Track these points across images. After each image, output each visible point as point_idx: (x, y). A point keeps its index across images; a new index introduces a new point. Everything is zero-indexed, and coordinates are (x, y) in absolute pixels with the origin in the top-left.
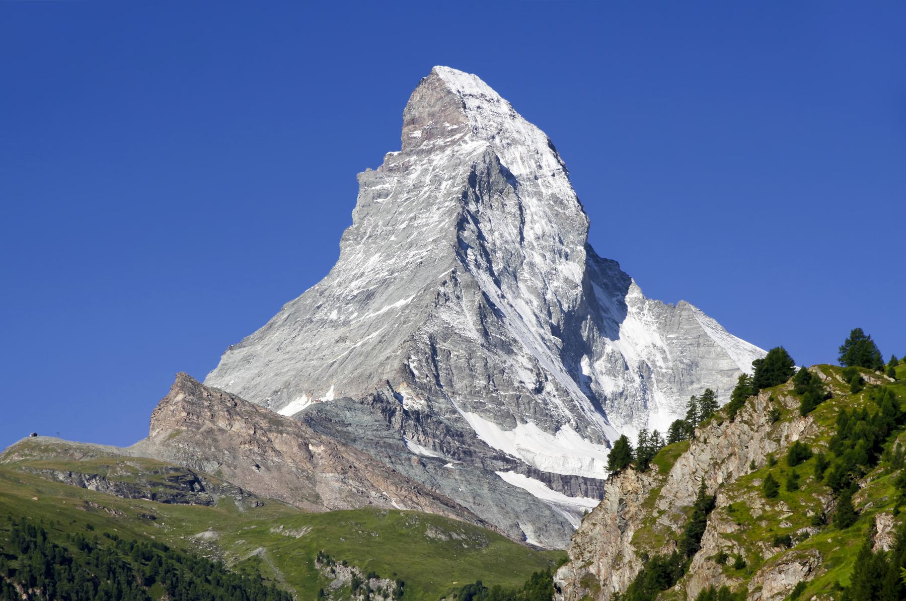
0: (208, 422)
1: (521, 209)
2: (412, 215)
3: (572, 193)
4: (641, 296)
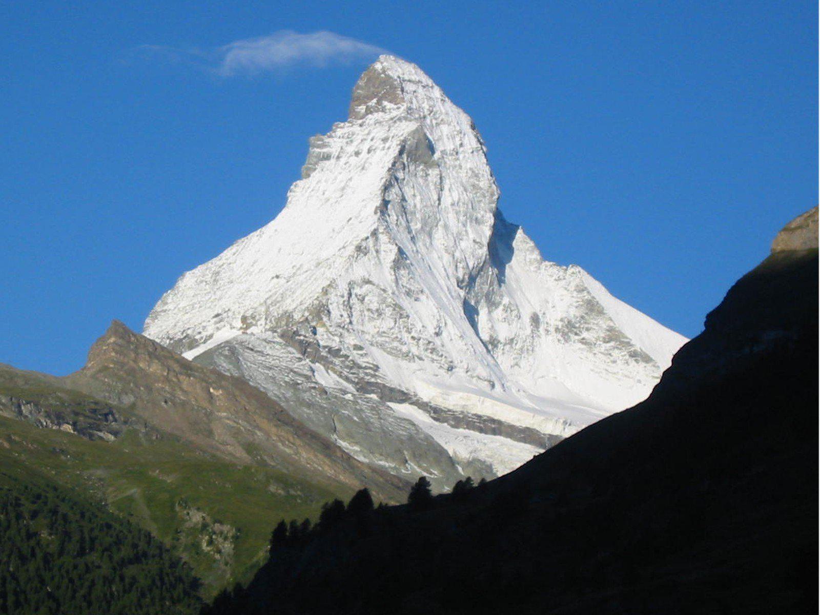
0: (131, 362)
3: (487, 168)
4: (539, 257)
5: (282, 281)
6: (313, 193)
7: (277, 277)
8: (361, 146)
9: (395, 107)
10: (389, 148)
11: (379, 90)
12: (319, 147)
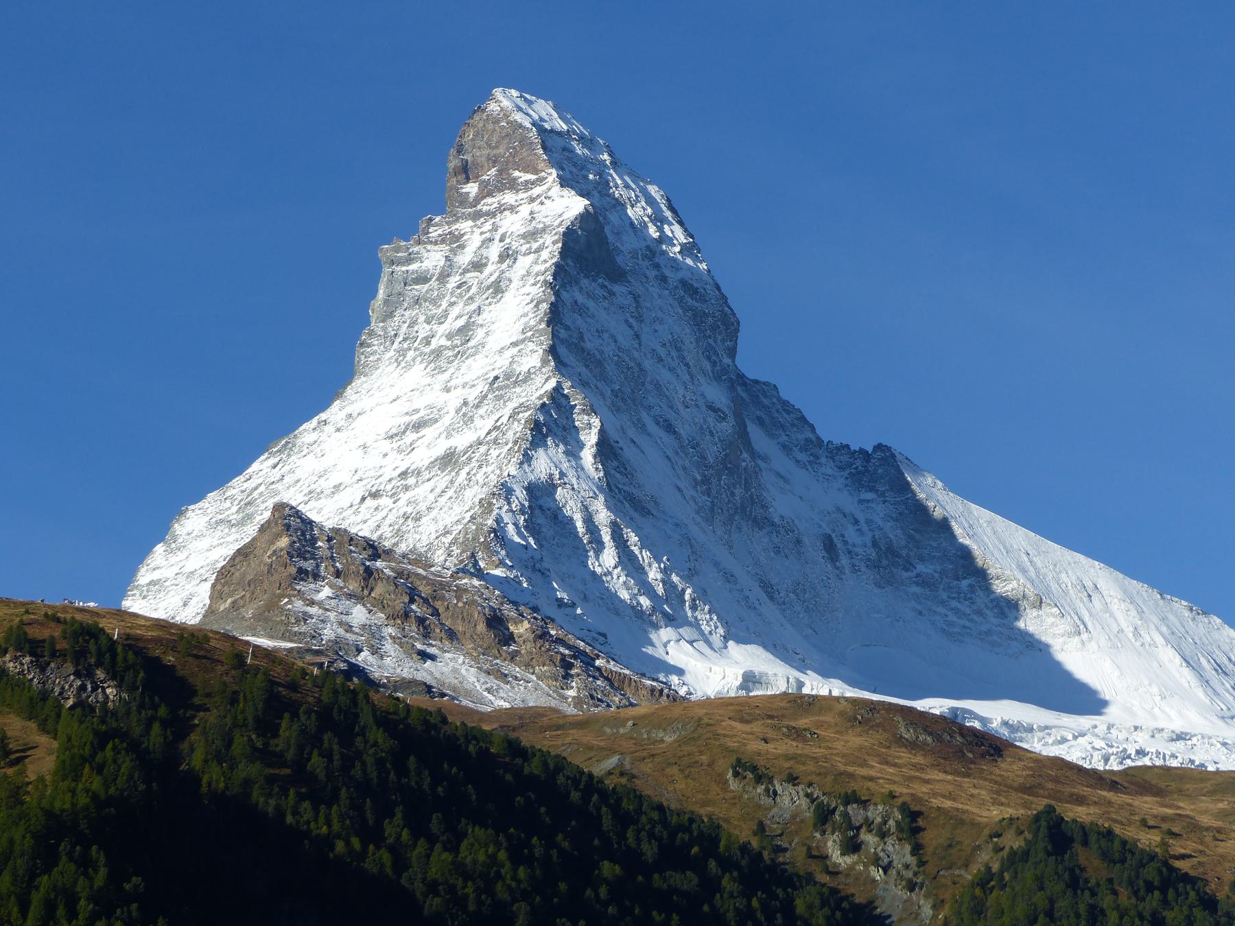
1: (636, 298)
2: (473, 307)
5: (385, 501)
6: (405, 345)
7: (375, 495)
8: (484, 252)
9: (533, 177)
10: (538, 251)
11: (501, 150)
12: (400, 262)
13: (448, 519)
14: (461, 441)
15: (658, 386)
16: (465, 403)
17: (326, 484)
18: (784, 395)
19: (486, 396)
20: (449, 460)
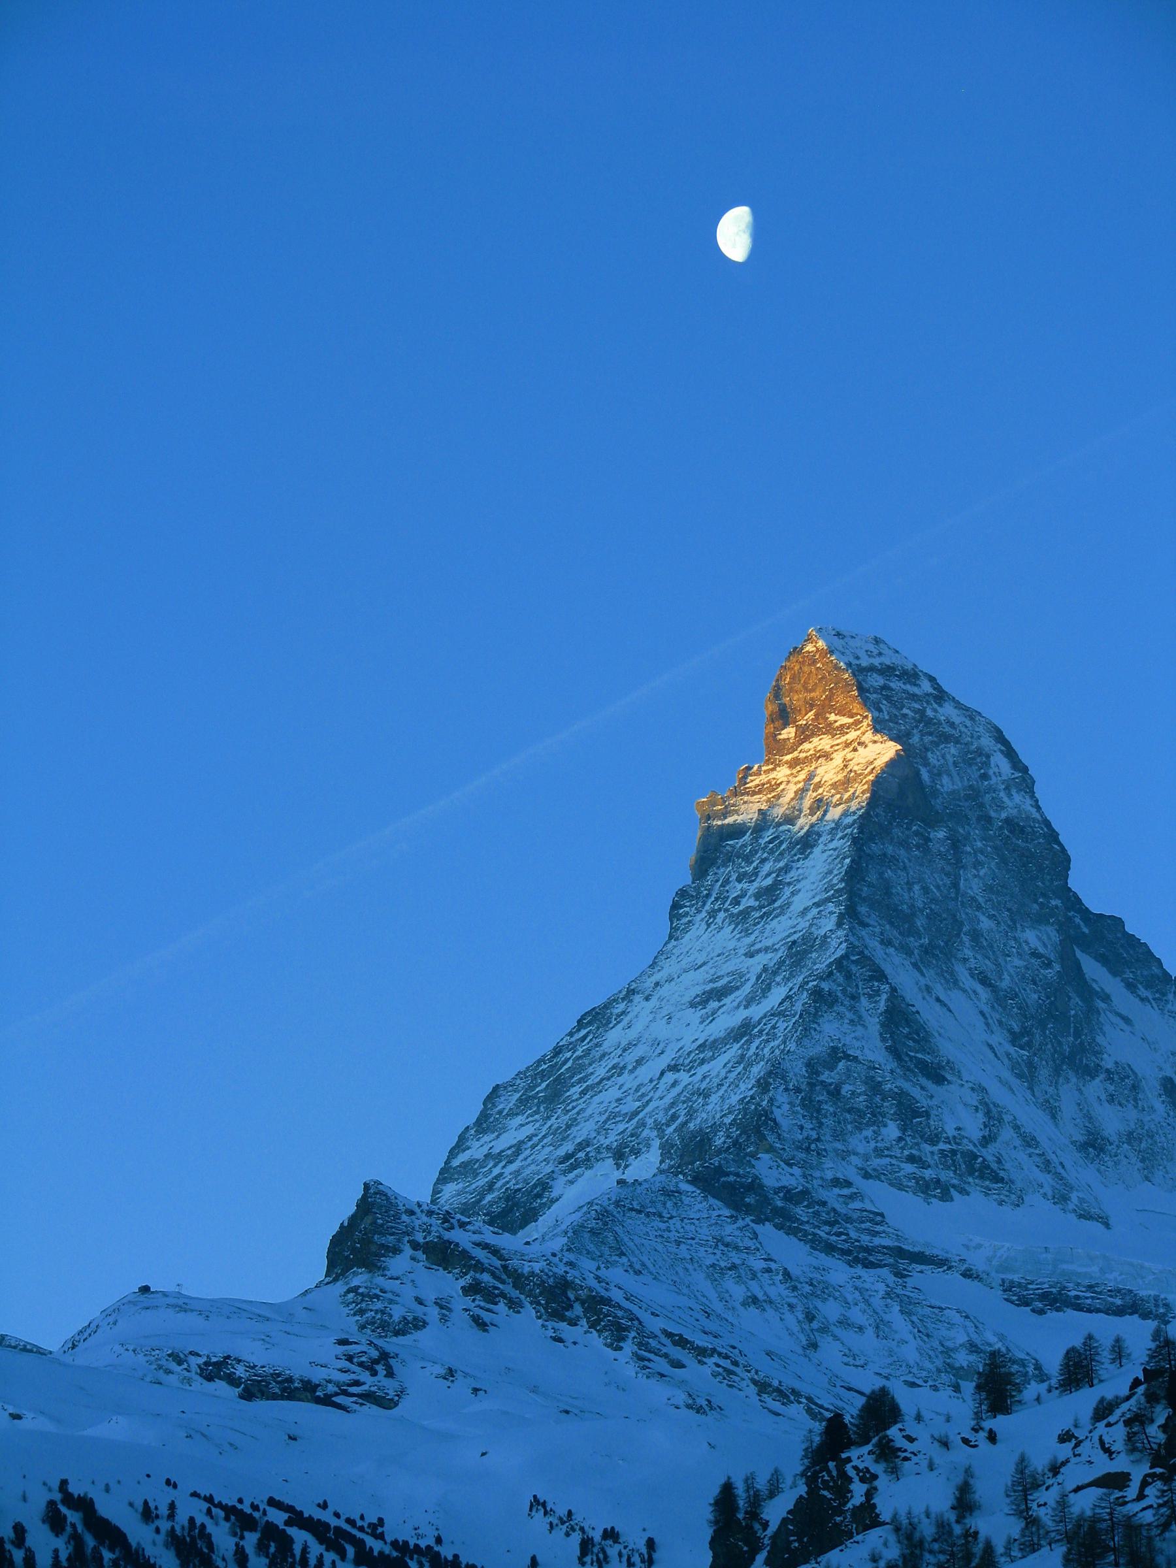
2: (781, 864)
5: (684, 1077)
7: (674, 1068)
9: (851, 720)
13: (734, 1099)
14: (756, 1012)
15: (976, 936)
16: (765, 969)
17: (631, 1058)
18: (1129, 929)
19: (784, 962)
20: (744, 1031)
